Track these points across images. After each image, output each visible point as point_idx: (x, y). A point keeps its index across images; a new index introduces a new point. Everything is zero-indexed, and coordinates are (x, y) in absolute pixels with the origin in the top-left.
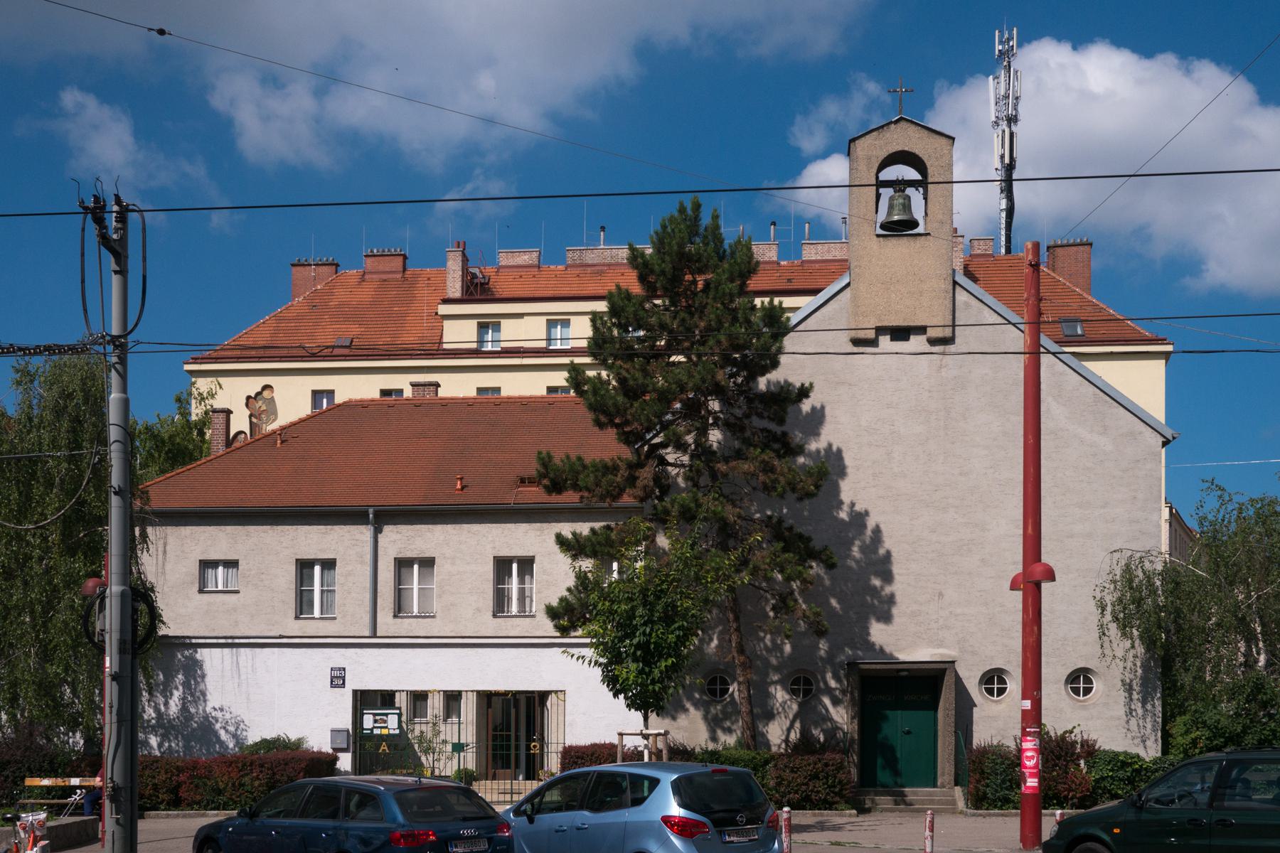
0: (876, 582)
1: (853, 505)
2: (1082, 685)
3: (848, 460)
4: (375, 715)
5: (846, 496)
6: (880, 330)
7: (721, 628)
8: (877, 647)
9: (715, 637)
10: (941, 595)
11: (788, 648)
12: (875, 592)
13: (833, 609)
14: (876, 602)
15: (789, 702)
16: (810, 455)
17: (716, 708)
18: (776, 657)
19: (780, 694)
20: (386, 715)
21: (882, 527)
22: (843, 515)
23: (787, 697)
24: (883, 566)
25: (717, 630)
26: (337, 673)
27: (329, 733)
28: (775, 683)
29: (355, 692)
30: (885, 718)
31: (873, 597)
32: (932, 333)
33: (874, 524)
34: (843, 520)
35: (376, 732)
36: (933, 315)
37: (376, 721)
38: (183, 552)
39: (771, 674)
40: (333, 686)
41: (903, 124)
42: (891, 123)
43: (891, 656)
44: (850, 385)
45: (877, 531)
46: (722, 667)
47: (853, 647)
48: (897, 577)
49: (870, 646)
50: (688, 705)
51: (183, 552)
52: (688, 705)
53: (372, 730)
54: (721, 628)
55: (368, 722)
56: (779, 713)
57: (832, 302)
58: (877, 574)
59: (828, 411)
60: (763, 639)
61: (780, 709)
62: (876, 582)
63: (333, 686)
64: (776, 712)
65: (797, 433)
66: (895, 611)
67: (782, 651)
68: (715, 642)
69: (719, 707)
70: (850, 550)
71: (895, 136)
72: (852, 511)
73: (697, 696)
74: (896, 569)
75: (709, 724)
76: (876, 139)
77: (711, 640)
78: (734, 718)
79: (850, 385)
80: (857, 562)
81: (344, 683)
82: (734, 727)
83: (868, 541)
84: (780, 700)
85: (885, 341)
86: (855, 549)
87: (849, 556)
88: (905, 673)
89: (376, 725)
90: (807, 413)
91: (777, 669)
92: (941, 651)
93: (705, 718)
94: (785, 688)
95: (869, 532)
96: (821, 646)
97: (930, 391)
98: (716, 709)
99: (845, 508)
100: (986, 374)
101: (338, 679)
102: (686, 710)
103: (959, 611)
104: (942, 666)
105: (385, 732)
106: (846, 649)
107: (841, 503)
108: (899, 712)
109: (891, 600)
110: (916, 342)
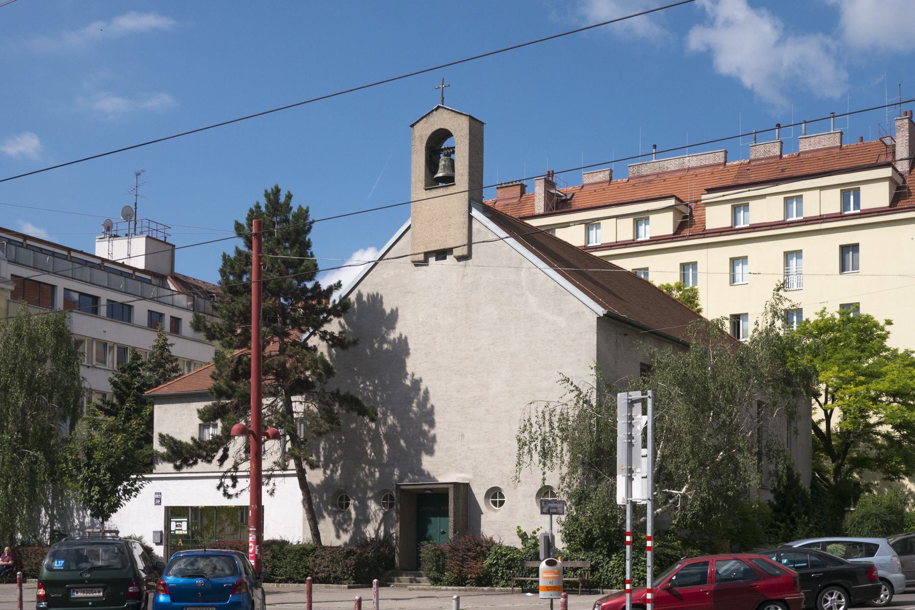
0: (426, 427)
1: (413, 375)
2: (498, 500)
3: (411, 345)
4: (176, 522)
5: (409, 370)
6: (427, 255)
7: (342, 462)
8: (426, 473)
9: (339, 468)
10: (463, 436)
11: (377, 475)
12: (425, 434)
13: (402, 447)
14: (425, 441)
15: (378, 511)
16: (389, 342)
17: (339, 516)
18: (371, 480)
19: (373, 506)
20: (181, 522)
21: (430, 390)
22: (408, 382)
23: (377, 508)
24: (428, 416)
25: (340, 464)
26: (157, 496)
27: (152, 534)
28: (370, 498)
29: (165, 507)
30: (430, 522)
31: (424, 438)
32: (457, 252)
33: (425, 388)
34: (407, 385)
35: (177, 532)
36: (455, 238)
37: (177, 526)
38: (191, 419)
39: (369, 493)
40: (156, 504)
41: (440, 110)
42: (433, 111)
43: (434, 479)
44: (413, 293)
45: (426, 392)
46: (342, 488)
47: (413, 474)
48: (437, 425)
49: (421, 472)
50: (325, 514)
51: (191, 419)
52: (325, 514)
53: (174, 531)
54: (342, 462)
55: (173, 526)
56: (372, 519)
57: (403, 238)
58: (426, 422)
59: (400, 312)
60: (363, 469)
61: (373, 516)
62: (426, 427)
63: (156, 504)
64: (371, 518)
65: (383, 328)
66: (436, 447)
67: (374, 476)
68: (339, 472)
69: (341, 515)
70: (412, 406)
71: (436, 119)
72: (413, 379)
73: (330, 508)
74: (437, 418)
75: (336, 527)
76: (425, 124)
77: (337, 470)
78: (348, 523)
79: (413, 293)
80: (416, 414)
81: (160, 502)
82: (349, 529)
83: (421, 398)
84: (373, 510)
85: (432, 260)
86: (414, 405)
87: (411, 411)
88: (429, 492)
89: (177, 528)
90: (389, 314)
91: (372, 489)
92: (463, 475)
93: (334, 522)
94: (377, 502)
95: (422, 393)
96: (395, 473)
97: (458, 294)
98: (339, 517)
99: (409, 377)
100: (490, 279)
101: (158, 501)
102: (324, 518)
103: (473, 447)
104: (446, 486)
105: (181, 532)
106: (409, 475)
107: (407, 374)
108: (438, 518)
109: (433, 439)
110: (450, 259)
